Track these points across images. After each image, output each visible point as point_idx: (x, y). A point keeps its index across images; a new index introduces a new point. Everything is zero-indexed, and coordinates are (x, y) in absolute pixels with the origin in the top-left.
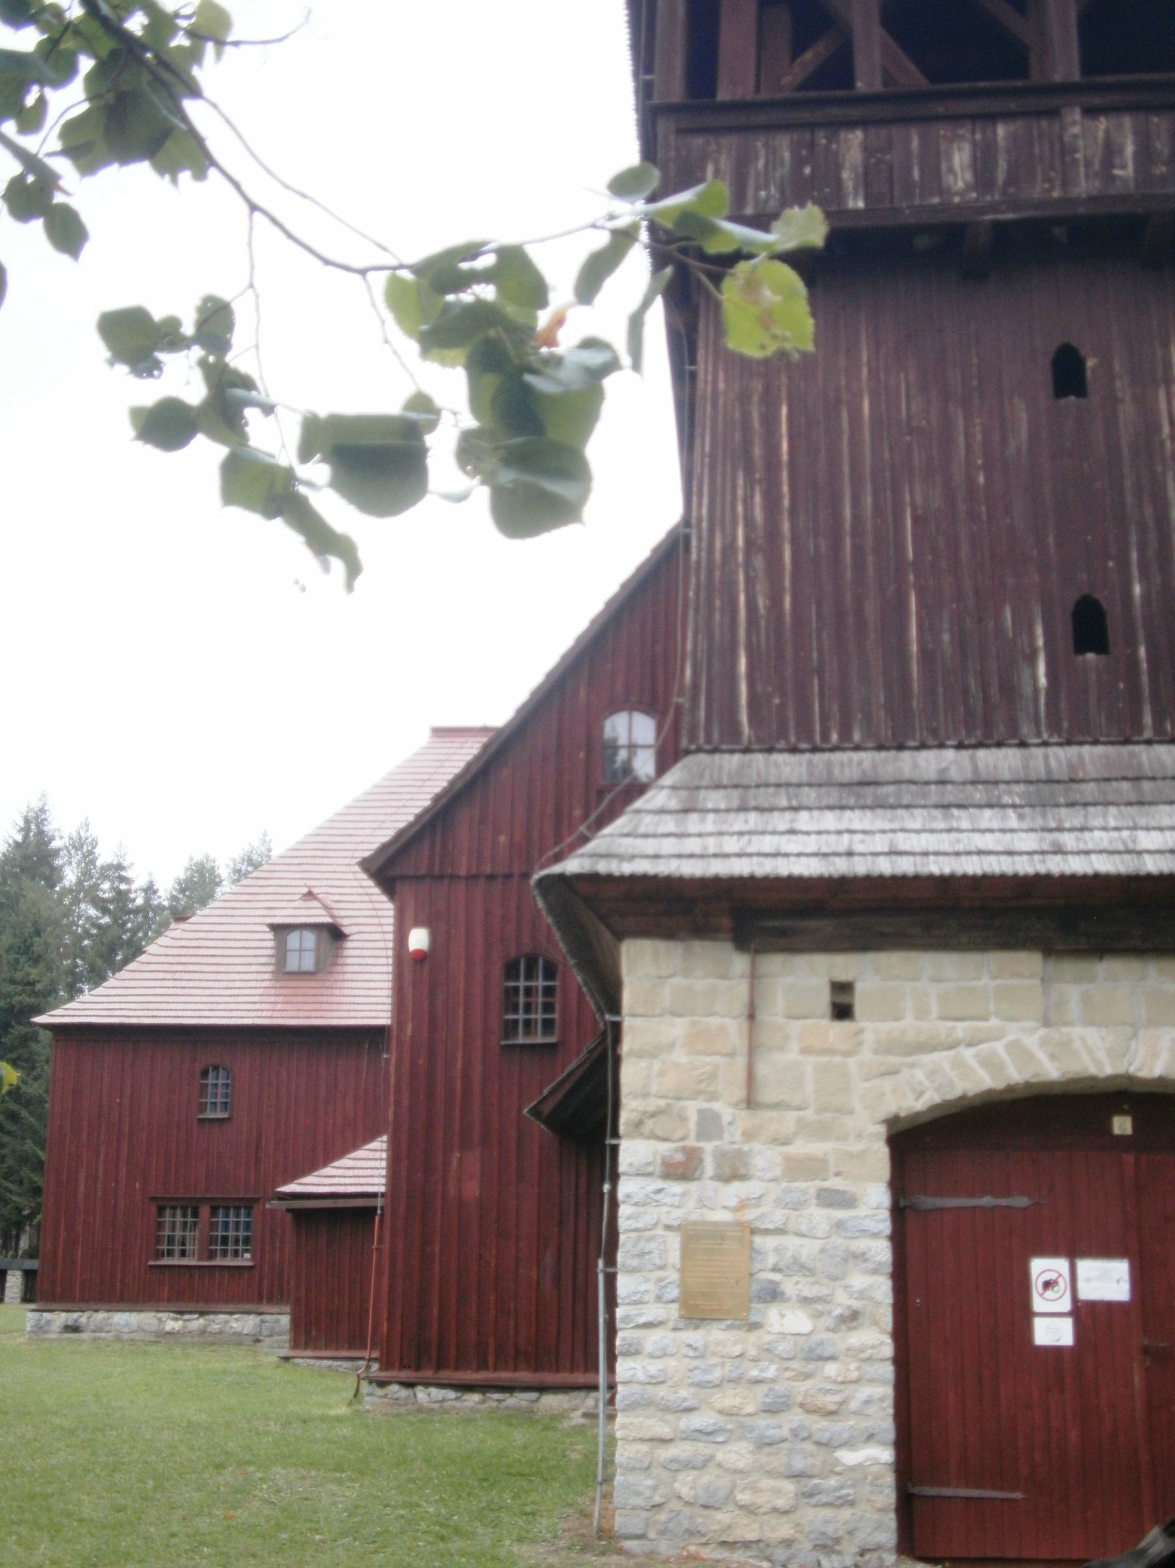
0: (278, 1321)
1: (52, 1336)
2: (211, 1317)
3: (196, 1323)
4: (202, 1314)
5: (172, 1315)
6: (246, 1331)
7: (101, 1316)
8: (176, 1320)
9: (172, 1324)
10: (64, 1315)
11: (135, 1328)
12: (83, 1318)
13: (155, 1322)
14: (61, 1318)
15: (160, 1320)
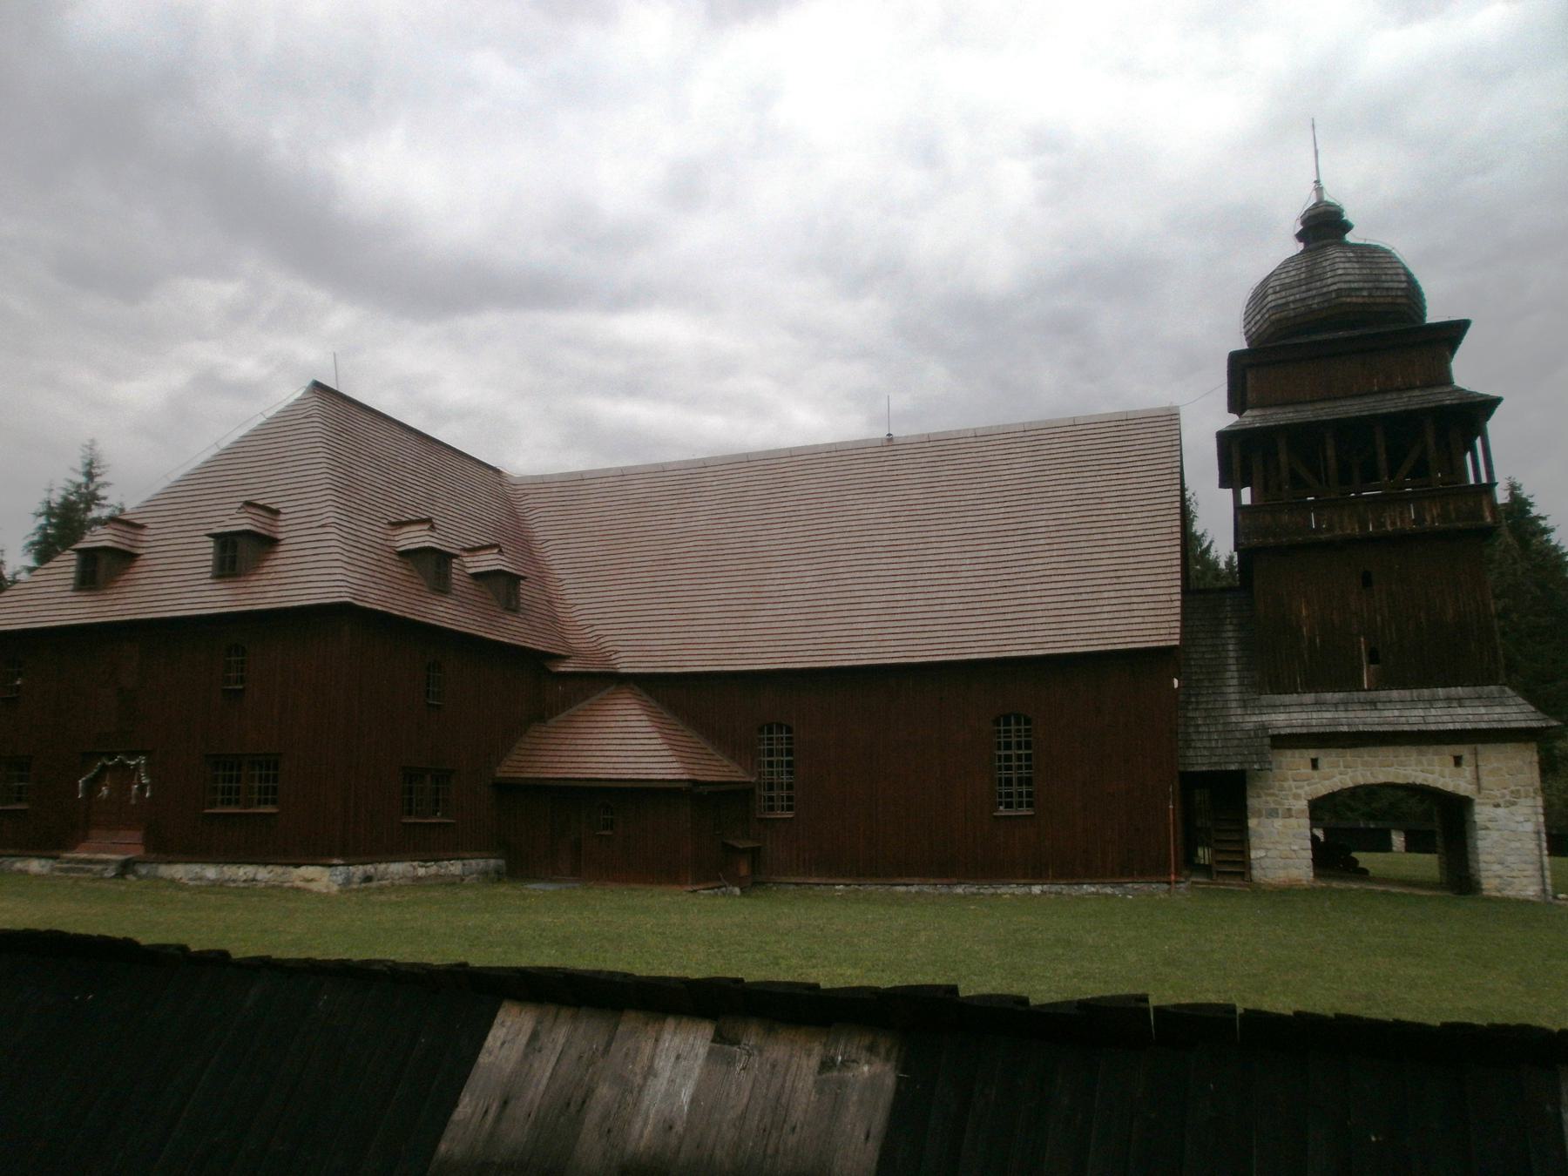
0: (470, 864)
1: (355, 886)
2: (440, 863)
3: (433, 868)
4: (436, 861)
5: (421, 864)
6: (457, 873)
7: (382, 867)
8: (422, 867)
9: (421, 872)
10: (361, 867)
11: (401, 876)
12: (370, 868)
13: (411, 869)
14: (358, 871)
15: (414, 868)
